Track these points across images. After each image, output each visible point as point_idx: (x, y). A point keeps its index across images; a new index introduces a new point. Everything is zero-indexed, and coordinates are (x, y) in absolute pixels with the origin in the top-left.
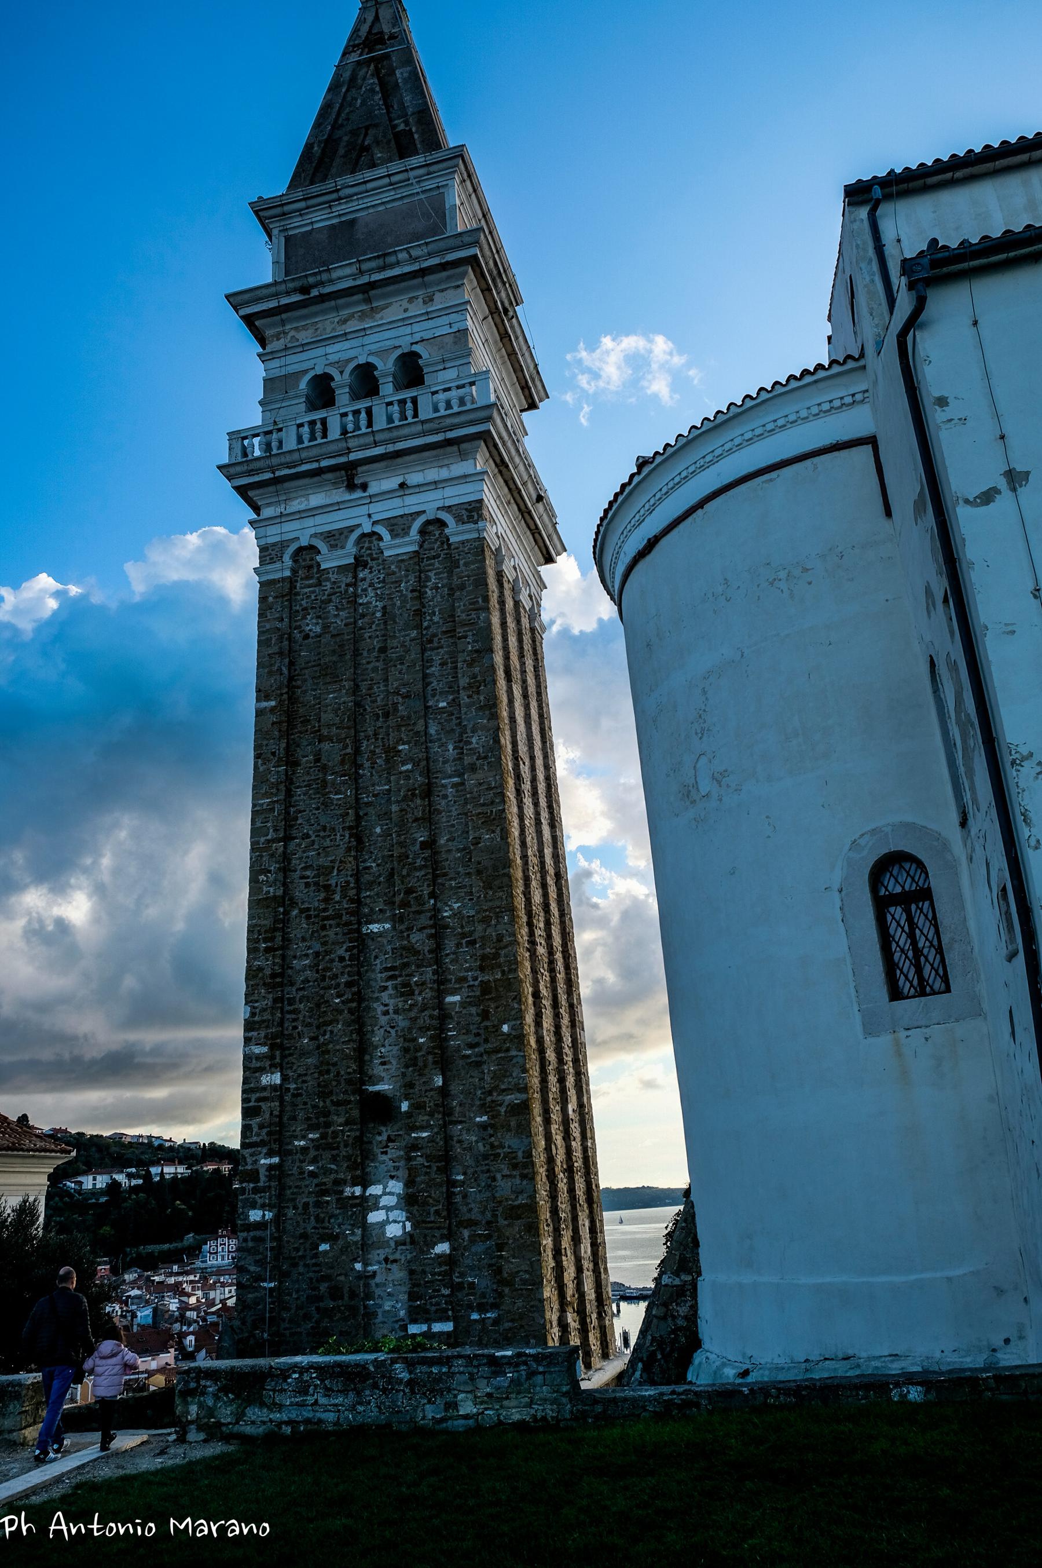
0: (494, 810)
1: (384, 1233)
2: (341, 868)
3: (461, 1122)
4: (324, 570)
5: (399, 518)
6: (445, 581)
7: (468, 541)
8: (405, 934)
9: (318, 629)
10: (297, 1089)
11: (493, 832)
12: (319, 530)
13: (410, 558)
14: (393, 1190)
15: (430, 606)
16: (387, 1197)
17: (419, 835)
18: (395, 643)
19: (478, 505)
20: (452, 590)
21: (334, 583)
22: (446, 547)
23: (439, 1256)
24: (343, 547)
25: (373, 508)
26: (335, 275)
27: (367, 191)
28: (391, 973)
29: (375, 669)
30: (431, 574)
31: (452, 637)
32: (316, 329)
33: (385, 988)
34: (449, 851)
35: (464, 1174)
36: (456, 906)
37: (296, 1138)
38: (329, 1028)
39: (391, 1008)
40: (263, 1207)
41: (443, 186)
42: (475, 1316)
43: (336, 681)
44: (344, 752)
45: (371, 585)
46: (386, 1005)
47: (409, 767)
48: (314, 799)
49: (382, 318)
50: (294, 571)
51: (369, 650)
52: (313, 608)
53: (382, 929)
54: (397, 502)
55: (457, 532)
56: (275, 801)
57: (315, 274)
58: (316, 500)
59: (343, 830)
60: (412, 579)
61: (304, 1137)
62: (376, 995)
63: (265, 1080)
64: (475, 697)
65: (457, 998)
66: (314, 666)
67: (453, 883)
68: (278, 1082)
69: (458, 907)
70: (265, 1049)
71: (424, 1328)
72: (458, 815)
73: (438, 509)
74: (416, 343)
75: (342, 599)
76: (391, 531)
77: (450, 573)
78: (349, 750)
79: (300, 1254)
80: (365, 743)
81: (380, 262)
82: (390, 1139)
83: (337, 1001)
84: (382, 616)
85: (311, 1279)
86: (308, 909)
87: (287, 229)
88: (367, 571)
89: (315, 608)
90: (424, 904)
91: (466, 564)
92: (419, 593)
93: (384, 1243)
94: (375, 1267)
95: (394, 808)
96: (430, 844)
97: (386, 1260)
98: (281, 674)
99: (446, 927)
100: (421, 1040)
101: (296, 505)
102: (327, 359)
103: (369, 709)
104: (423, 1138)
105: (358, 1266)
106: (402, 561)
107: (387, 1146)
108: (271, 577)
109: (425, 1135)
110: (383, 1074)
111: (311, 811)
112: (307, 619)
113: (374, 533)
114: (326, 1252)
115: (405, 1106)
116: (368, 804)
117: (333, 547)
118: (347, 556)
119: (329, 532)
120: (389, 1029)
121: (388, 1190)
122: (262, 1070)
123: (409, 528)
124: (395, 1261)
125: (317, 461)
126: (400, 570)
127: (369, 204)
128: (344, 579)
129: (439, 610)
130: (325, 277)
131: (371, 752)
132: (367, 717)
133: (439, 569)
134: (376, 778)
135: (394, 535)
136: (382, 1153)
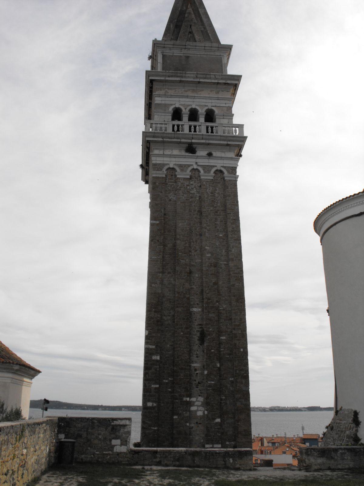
0: (240, 275)
1: (196, 414)
2: (184, 287)
3: (225, 380)
4: (178, 178)
5: (207, 166)
6: (222, 192)
7: (231, 180)
8: (207, 313)
9: (175, 198)
11: (239, 283)
12: (177, 163)
13: (211, 181)
14: (200, 400)
16: (198, 402)
18: (205, 210)
19: (235, 169)
20: (225, 197)
21: (182, 183)
22: (222, 180)
23: (217, 423)
24: (186, 171)
25: (198, 160)
26: (187, 75)
27: (195, 49)
28: (201, 326)
30: (217, 188)
31: (224, 212)
32: (176, 91)
35: (225, 397)
36: (224, 306)
37: (164, 379)
38: (179, 342)
40: (153, 402)
42: (227, 443)
44: (185, 245)
45: (195, 187)
47: (210, 255)
49: (200, 94)
50: (166, 176)
51: (194, 210)
52: (172, 190)
53: (197, 310)
54: (206, 160)
56: (159, 258)
57: (180, 73)
58: (176, 152)
59: (185, 273)
61: (167, 379)
65: (224, 338)
66: (173, 212)
67: (224, 298)
69: (225, 307)
70: (154, 347)
72: (226, 275)
73: (221, 166)
74: (213, 106)
76: (204, 170)
78: (187, 245)
80: (192, 243)
81: (205, 76)
82: (199, 383)
83: (182, 333)
84: (199, 199)
87: (164, 52)
88: (193, 182)
89: (174, 191)
94: (193, 425)
95: (204, 269)
96: (216, 284)
97: (197, 423)
98: (161, 212)
100: (213, 351)
101: (167, 152)
102: (180, 103)
103: (194, 232)
104: (212, 384)
105: (188, 424)
106: (207, 181)
107: (198, 385)
108: (157, 176)
109: (213, 382)
113: (197, 169)
114: (176, 419)
118: (188, 175)
119: (181, 165)
121: (198, 400)
123: (211, 170)
124: (200, 424)
126: (207, 184)
129: (220, 202)
130: (184, 75)
131: (195, 247)
132: (193, 234)
133: (220, 187)
135: (205, 172)
136: (196, 387)
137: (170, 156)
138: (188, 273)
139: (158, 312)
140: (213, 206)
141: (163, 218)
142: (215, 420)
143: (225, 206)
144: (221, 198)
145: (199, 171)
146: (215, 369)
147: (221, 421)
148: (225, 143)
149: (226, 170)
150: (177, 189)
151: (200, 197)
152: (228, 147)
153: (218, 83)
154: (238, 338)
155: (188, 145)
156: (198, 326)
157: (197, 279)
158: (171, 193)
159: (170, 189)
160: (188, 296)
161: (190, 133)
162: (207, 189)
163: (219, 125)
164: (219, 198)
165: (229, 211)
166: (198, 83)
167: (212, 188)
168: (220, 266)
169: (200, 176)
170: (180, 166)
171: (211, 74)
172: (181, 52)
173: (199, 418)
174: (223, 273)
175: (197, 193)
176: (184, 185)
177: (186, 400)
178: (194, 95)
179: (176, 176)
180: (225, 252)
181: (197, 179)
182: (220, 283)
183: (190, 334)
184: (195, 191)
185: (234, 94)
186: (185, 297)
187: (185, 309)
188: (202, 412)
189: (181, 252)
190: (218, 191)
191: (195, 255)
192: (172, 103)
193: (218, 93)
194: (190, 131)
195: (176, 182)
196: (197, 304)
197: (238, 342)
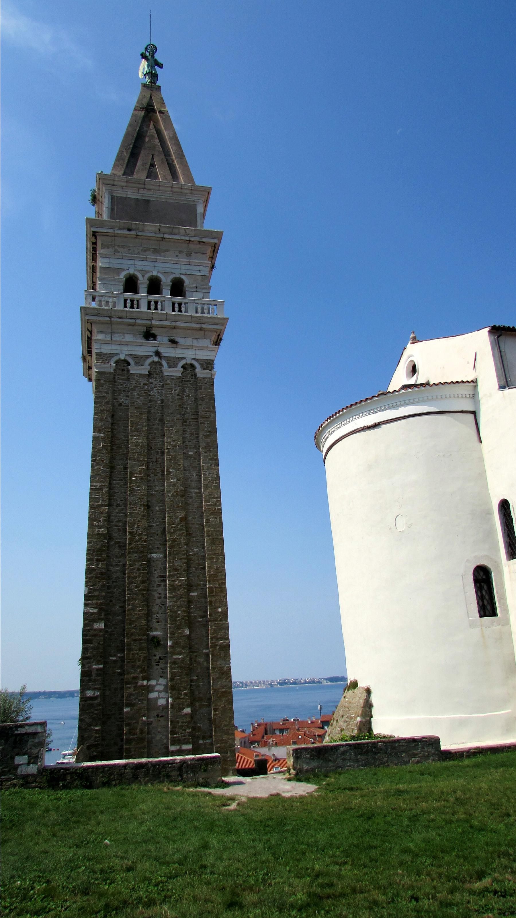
0: (216, 508)
1: (157, 703)
3: (196, 652)
4: (131, 374)
6: (193, 394)
7: (206, 378)
9: (127, 402)
10: (111, 631)
11: (216, 518)
14: (162, 683)
15: (185, 404)
17: (180, 514)
19: (212, 362)
21: (137, 381)
22: (194, 378)
23: (186, 714)
28: (162, 579)
29: (157, 429)
30: (186, 389)
31: (196, 422)
32: (129, 250)
33: (160, 586)
34: (193, 524)
35: (197, 676)
36: (196, 550)
37: (111, 656)
38: (132, 602)
39: (162, 595)
40: (94, 689)
41: (197, 202)
42: (201, 742)
43: (138, 431)
45: (155, 387)
46: (160, 594)
48: (123, 487)
49: (164, 256)
50: (115, 370)
52: (124, 391)
53: (158, 557)
55: (200, 372)
58: (128, 338)
60: (178, 389)
61: (115, 656)
62: (155, 588)
63: (96, 626)
64: (209, 453)
65: (196, 594)
68: (103, 627)
69: (197, 551)
70: (96, 610)
71: (178, 747)
73: (192, 359)
75: (142, 390)
76: (168, 363)
77: (196, 391)
79: (112, 713)
80: (151, 465)
82: (160, 659)
83: (136, 589)
85: (118, 725)
86: (119, 542)
88: (153, 380)
89: (125, 391)
90: (182, 547)
91: (205, 389)
92: (181, 395)
93: (157, 708)
95: (166, 499)
96: (184, 519)
97: (158, 716)
99: (191, 559)
101: (117, 338)
102: (135, 267)
103: (153, 448)
104: (179, 659)
105: (145, 718)
106: (173, 379)
107: (159, 662)
110: (157, 627)
111: (121, 493)
112: (120, 396)
114: (127, 712)
115: (169, 643)
116: (152, 495)
117: (137, 363)
119: (135, 355)
120: (161, 606)
121: (159, 683)
122: (95, 621)
123: (177, 364)
124: (162, 716)
125: (134, 319)
127: (158, 196)
128: (143, 380)
131: (154, 469)
132: (153, 452)
134: (156, 483)
135: (169, 367)
136: (156, 665)
137: (120, 344)
138: (144, 505)
139: (103, 561)
140: (180, 413)
141: (110, 430)
142: (183, 710)
143: (197, 413)
144: (192, 401)
145: (161, 365)
146: (183, 638)
147: (192, 711)
148: (198, 326)
149: (199, 363)
150: (131, 389)
151: (162, 400)
152: (203, 332)
153: (190, 241)
154: (214, 594)
155: (147, 327)
156: (159, 579)
157: (158, 513)
158: (122, 395)
159: (120, 389)
160: (146, 537)
161: (149, 311)
162: (173, 389)
163: (190, 301)
164: (189, 402)
165: (201, 420)
166: (161, 239)
167: (180, 389)
168: (189, 496)
169: (162, 372)
170: (135, 357)
171: (179, 228)
172: (139, 193)
173: (161, 709)
174: (194, 505)
175: (158, 395)
176: (140, 384)
177: (143, 683)
178: (156, 257)
179: (128, 371)
180: (197, 475)
181: (157, 376)
182: (190, 518)
183: (148, 590)
184: (156, 392)
185: (212, 258)
186: (141, 539)
187: (141, 556)
188: (165, 699)
189: (135, 477)
190: (187, 392)
191: (154, 481)
192: (123, 267)
193: (190, 256)
194: (149, 308)
195: (128, 379)
196: (158, 548)
197: (214, 599)
